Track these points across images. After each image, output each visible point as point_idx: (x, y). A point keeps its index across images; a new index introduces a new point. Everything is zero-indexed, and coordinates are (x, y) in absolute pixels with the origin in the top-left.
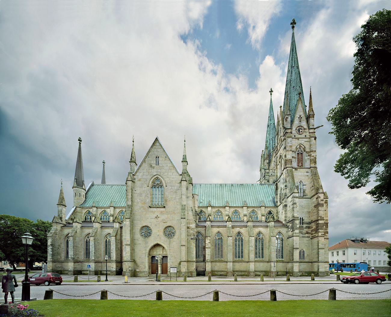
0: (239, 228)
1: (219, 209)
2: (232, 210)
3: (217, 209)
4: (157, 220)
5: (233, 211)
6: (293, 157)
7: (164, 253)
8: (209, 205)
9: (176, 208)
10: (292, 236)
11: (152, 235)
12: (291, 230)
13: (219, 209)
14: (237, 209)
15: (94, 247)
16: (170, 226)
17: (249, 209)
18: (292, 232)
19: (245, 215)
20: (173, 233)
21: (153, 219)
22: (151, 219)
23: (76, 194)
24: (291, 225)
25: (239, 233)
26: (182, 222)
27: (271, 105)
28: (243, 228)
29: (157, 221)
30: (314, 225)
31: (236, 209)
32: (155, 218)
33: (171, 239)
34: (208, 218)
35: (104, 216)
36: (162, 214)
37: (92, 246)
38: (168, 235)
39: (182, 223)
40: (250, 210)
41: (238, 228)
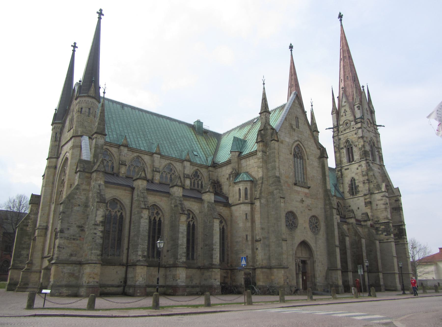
4: (303, 205)
9: (318, 191)
10: (386, 241)
12: (385, 233)
15: (186, 236)
18: (385, 235)
23: (91, 112)
24: (383, 227)
27: (291, 75)
29: (302, 207)
35: (166, 174)
37: (182, 233)
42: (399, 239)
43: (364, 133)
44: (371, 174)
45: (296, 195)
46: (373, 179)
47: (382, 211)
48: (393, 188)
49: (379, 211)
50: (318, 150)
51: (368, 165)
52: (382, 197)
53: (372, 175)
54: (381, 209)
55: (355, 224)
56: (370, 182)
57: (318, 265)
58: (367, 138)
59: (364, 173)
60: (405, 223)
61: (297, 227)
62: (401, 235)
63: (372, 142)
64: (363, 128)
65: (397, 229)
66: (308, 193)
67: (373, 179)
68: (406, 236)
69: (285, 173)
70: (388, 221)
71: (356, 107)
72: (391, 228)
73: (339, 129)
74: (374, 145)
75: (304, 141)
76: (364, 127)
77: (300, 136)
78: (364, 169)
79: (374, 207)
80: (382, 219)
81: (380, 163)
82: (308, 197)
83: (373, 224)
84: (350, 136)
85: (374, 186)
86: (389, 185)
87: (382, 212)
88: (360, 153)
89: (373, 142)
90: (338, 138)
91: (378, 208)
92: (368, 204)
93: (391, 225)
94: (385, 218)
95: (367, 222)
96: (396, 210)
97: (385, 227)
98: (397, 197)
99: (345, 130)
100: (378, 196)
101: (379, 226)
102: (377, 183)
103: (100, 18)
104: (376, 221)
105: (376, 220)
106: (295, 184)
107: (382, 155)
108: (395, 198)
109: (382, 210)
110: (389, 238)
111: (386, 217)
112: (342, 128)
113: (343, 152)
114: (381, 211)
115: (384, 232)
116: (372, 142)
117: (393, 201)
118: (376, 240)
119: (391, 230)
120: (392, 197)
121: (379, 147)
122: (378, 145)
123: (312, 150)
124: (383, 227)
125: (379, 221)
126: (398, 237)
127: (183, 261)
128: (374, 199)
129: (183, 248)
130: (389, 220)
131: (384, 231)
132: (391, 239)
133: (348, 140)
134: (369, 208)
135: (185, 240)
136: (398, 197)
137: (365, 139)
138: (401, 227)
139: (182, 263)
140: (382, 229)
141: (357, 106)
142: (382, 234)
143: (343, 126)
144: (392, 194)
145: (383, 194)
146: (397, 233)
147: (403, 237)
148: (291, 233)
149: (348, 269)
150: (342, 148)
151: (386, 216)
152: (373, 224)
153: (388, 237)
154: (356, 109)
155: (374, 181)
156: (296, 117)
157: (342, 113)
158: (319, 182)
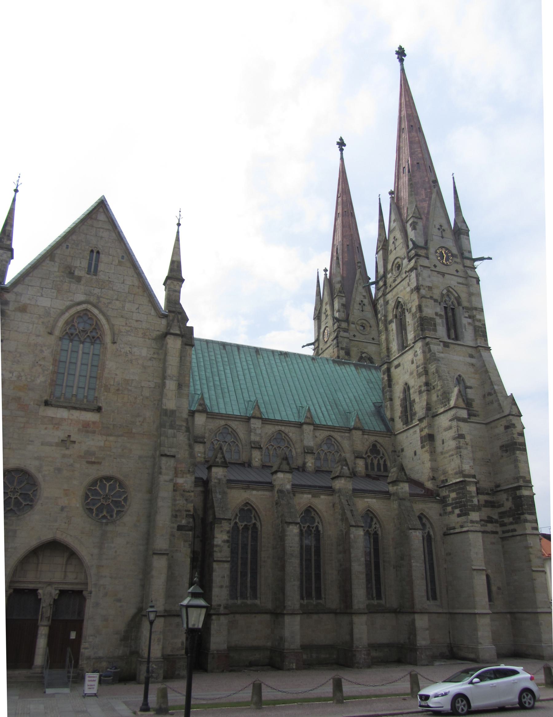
0: (310, 496)
1: (230, 423)
2: (270, 429)
3: (223, 423)
4: (67, 452)
5: (270, 432)
6: (436, 314)
7: (71, 577)
8: (201, 408)
11: (38, 507)
12: (457, 511)
13: (230, 423)
14: (283, 428)
16: (108, 479)
17: (318, 433)
19: (308, 451)
20: (117, 504)
21: (52, 446)
22: (42, 444)
24: (453, 495)
25: (309, 511)
26: (163, 467)
28: (322, 497)
29: (64, 456)
30: (507, 500)
31: (279, 428)
32: (57, 445)
33: (110, 528)
34: (220, 455)
36: (87, 432)
38: (100, 509)
39: (164, 471)
40: (322, 435)
41: (305, 496)
42: (516, 523)
43: (420, 278)
44: (432, 370)
45: (46, 429)
46: (438, 384)
47: (452, 455)
48: (501, 399)
49: (447, 455)
50: (159, 319)
51: (427, 350)
52: (451, 420)
53: (435, 371)
54: (450, 450)
55: (350, 492)
56: (432, 388)
57: (97, 604)
58: (430, 288)
59: (421, 370)
60: (533, 483)
61: (31, 506)
62: (519, 512)
63: (452, 297)
64: (419, 268)
65: (510, 498)
66: (94, 423)
67: (435, 382)
68: (534, 513)
69: (14, 379)
70: (461, 479)
71: (408, 225)
72: (473, 497)
73: (388, 281)
74: (459, 304)
75: (106, 301)
76: (421, 266)
77: (97, 291)
78: (419, 360)
79: (439, 448)
80: (452, 474)
81: (477, 343)
82: (94, 432)
83: (436, 488)
84: (401, 291)
85: (438, 396)
86: (493, 392)
87: (452, 458)
88: (414, 324)
89: (456, 298)
90: (384, 301)
91: (445, 449)
92: (425, 442)
93: (472, 489)
94: (456, 473)
95: (397, 485)
96: (507, 451)
97: (457, 494)
98: (508, 418)
99: (395, 281)
100: (444, 421)
101: (447, 493)
102: (442, 388)
104: (443, 481)
105: (442, 478)
106: (47, 403)
107: (484, 325)
108: (504, 422)
109: (451, 453)
110: (464, 522)
111: (457, 470)
112: (391, 277)
113: (392, 330)
114: (450, 456)
115: (456, 508)
116: (452, 297)
117: (502, 429)
118: (411, 529)
119: (472, 501)
120: (498, 419)
121: (474, 306)
122: (470, 301)
123: (137, 321)
124: (453, 495)
125: (447, 480)
126: (514, 519)
128: (438, 427)
130: (465, 476)
131: (458, 504)
132: (470, 525)
133: (400, 302)
134: (426, 451)
136: (511, 417)
137: (423, 292)
138: (518, 493)
140: (453, 499)
141: (410, 222)
142: (452, 512)
143: (392, 273)
144: (499, 413)
145: (453, 412)
146: (510, 508)
147: (522, 517)
149: (285, 607)
150: (391, 321)
151: (459, 468)
152: (436, 488)
153: (463, 519)
154: (409, 229)
155: (437, 385)
156: (92, 251)
157: (391, 247)
158: (147, 393)
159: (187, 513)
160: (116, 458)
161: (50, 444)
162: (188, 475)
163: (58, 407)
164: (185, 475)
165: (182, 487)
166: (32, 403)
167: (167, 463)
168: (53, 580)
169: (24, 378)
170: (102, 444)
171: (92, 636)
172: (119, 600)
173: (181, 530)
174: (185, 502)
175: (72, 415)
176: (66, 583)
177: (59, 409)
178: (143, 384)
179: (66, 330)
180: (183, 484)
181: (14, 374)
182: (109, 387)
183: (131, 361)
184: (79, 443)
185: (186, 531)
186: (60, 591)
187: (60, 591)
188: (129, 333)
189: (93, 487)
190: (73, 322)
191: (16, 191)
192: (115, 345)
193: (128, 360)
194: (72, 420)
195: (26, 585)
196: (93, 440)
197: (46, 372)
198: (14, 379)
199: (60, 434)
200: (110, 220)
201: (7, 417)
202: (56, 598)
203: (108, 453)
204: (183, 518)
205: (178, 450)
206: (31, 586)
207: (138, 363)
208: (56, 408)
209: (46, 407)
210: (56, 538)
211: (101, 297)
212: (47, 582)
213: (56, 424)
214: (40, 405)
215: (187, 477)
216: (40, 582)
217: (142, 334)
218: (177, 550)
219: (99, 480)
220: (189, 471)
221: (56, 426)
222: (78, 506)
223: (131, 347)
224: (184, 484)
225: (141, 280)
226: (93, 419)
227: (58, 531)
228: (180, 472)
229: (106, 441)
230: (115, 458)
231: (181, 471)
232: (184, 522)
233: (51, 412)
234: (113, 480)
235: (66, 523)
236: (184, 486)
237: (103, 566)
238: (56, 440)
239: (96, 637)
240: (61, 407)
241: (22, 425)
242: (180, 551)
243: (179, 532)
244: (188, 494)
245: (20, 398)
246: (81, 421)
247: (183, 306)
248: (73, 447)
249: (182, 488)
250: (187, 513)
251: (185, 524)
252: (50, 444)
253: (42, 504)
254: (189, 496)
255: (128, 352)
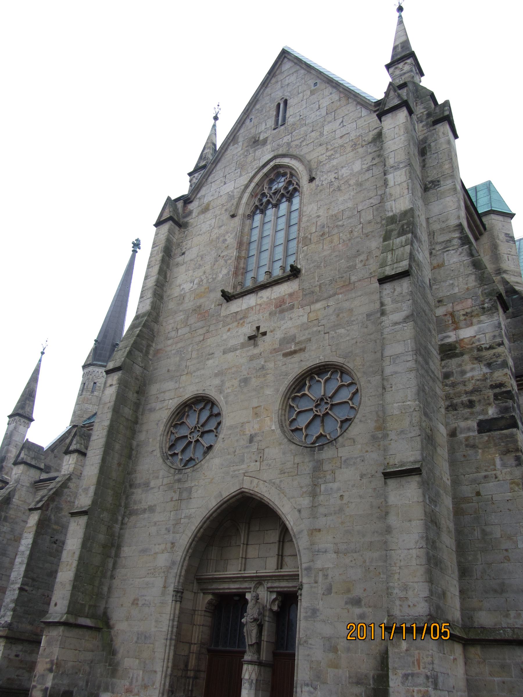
4: (256, 351)
15: (26, 561)
22: (224, 353)
29: (252, 358)
45: (229, 330)
57: (314, 612)
66: (291, 295)
69: (195, 286)
82: (292, 307)
103: (135, 252)
123: (341, 137)
127: (6, 621)
129: (14, 590)
135: (23, 568)
139: (3, 627)
148: (179, 481)
159: (497, 390)
160: (328, 333)
161: (233, 349)
162: (482, 318)
163: (243, 296)
164: (475, 320)
165: (473, 343)
166: (213, 306)
167: (395, 290)
168: (262, 572)
169: (205, 281)
170: (305, 319)
171: (307, 685)
172: (357, 602)
173: (489, 430)
174: (486, 370)
175: (262, 297)
176: (283, 576)
177: (244, 297)
178: (360, 208)
179: (255, 203)
180: (475, 336)
181: (195, 282)
182: (309, 237)
183: (339, 189)
184: (271, 331)
185: (502, 430)
186: (279, 593)
187: (279, 593)
188: (333, 157)
189: (298, 391)
190: (263, 190)
191: (216, 118)
192: (314, 182)
193: (334, 190)
194: (261, 305)
195: (226, 586)
196: (291, 319)
197: (229, 262)
198: (195, 286)
199: (248, 330)
200: (295, 61)
201: (186, 335)
202: (275, 608)
203: (315, 329)
204: (489, 404)
205: (451, 282)
206: (234, 587)
207: (350, 185)
208: (241, 299)
209: (228, 303)
210: (243, 490)
211: (292, 142)
212: (253, 577)
213: (241, 319)
214: (221, 305)
215: (480, 322)
216: (244, 579)
217: (352, 146)
218: (485, 477)
219: (308, 379)
220: (483, 308)
221: (241, 321)
222: (273, 428)
223: (336, 171)
224: (478, 337)
225: (341, 89)
226: (290, 291)
227: (245, 478)
228: (462, 318)
229: (310, 312)
230: (326, 333)
231: (464, 315)
232: (492, 412)
233: (236, 306)
234: (329, 371)
235: (256, 461)
236: (479, 340)
237: (320, 530)
238: (242, 339)
239: (315, 689)
240: (245, 295)
241: (201, 338)
242: (496, 478)
243: (485, 437)
244: (492, 352)
245: (200, 306)
246: (274, 301)
247: (428, 88)
248: (264, 341)
249: (474, 345)
250: (497, 390)
251: (495, 416)
252: (233, 349)
253: (223, 438)
254: (494, 355)
255: (333, 180)
